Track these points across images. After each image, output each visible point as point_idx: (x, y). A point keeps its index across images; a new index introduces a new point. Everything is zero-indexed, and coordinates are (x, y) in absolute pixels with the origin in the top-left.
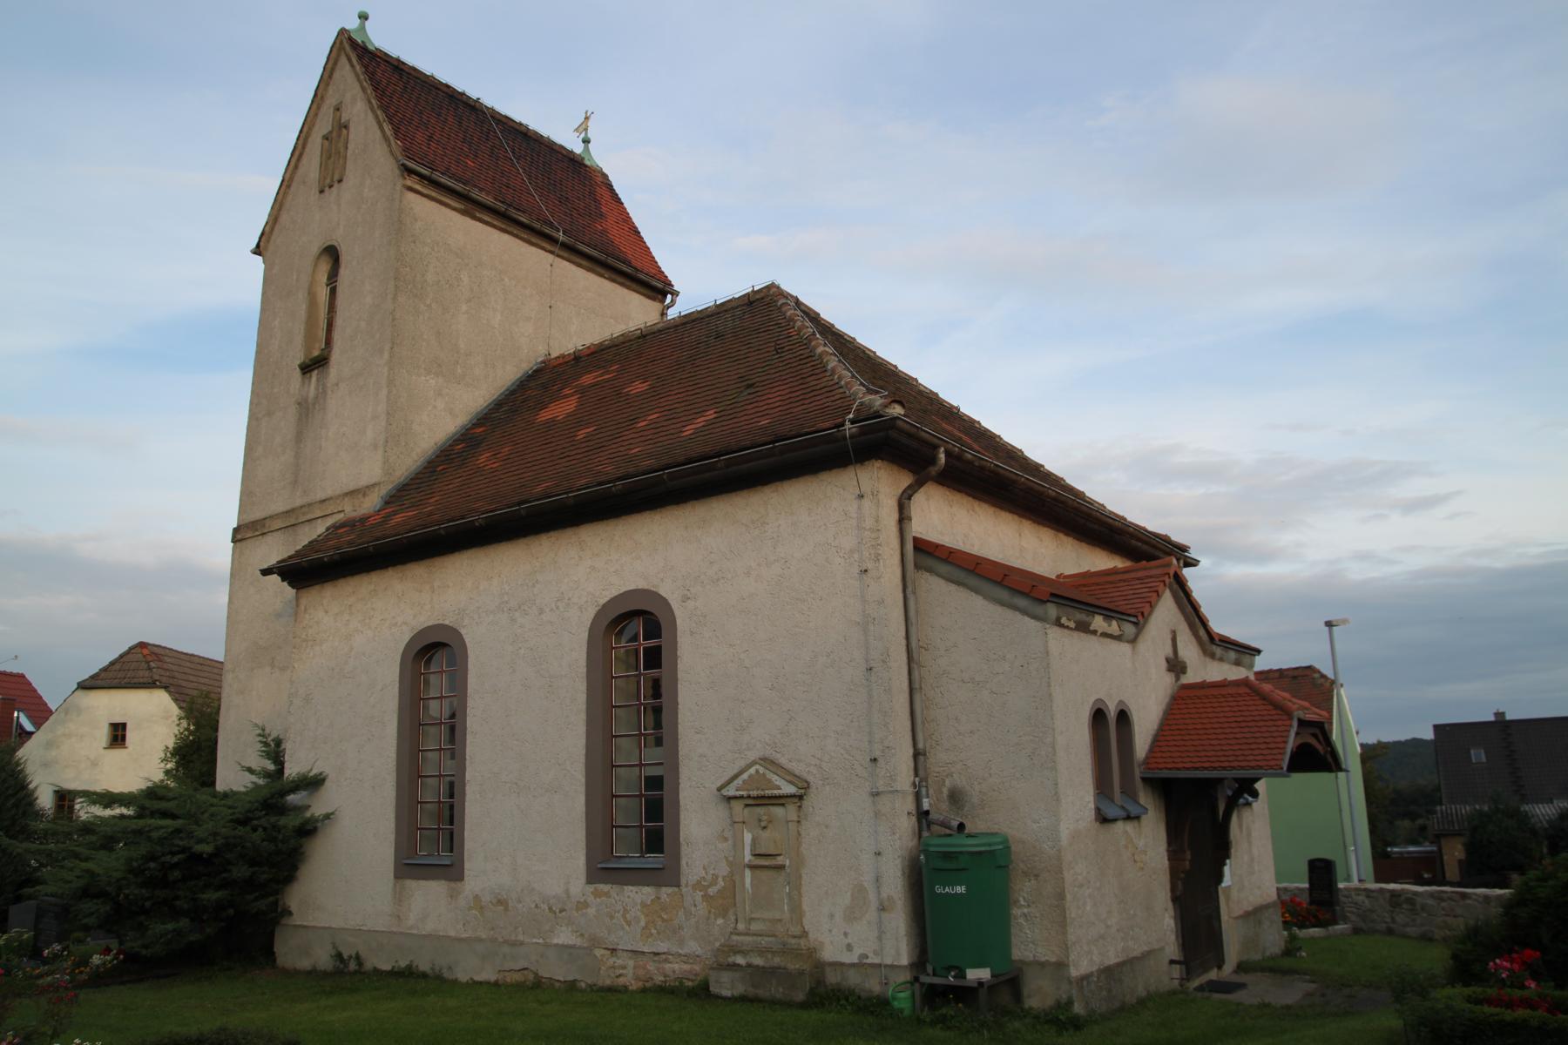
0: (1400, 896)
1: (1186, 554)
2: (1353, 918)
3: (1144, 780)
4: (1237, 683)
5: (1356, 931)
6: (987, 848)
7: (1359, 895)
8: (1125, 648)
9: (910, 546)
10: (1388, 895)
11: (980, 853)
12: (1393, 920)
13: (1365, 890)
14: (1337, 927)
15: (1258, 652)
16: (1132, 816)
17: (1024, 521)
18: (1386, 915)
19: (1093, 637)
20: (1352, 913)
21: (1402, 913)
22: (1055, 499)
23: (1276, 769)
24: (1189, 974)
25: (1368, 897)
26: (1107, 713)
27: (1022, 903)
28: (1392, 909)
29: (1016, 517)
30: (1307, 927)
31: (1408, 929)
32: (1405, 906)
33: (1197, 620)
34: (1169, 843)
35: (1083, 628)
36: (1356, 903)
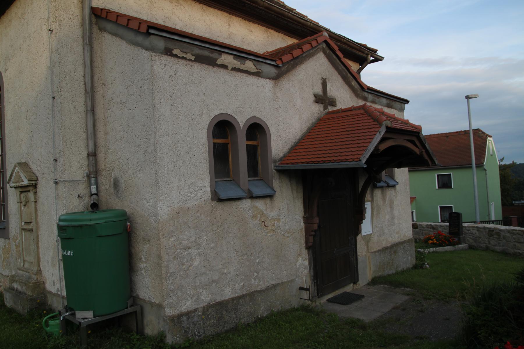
0: (493, 231)
1: (377, 54)
2: (471, 240)
3: (279, 171)
4: (358, 108)
5: (471, 247)
6: (88, 223)
7: (473, 230)
8: (268, 84)
9: (87, 11)
10: (487, 230)
11: (81, 226)
12: (489, 243)
13: (477, 227)
14: (460, 246)
15: (407, 102)
16: (254, 196)
17: (234, 17)
18: (486, 240)
19: (222, 71)
20: (470, 238)
21: (494, 239)
22: (266, 8)
23: (350, 162)
24: (321, 291)
25: (478, 231)
26: (236, 126)
27: (143, 260)
28: (489, 237)
29: (225, 14)
30: (444, 246)
31: (496, 248)
32: (495, 236)
33: (349, 75)
34: (305, 212)
35: (168, 52)
36: (472, 234)
